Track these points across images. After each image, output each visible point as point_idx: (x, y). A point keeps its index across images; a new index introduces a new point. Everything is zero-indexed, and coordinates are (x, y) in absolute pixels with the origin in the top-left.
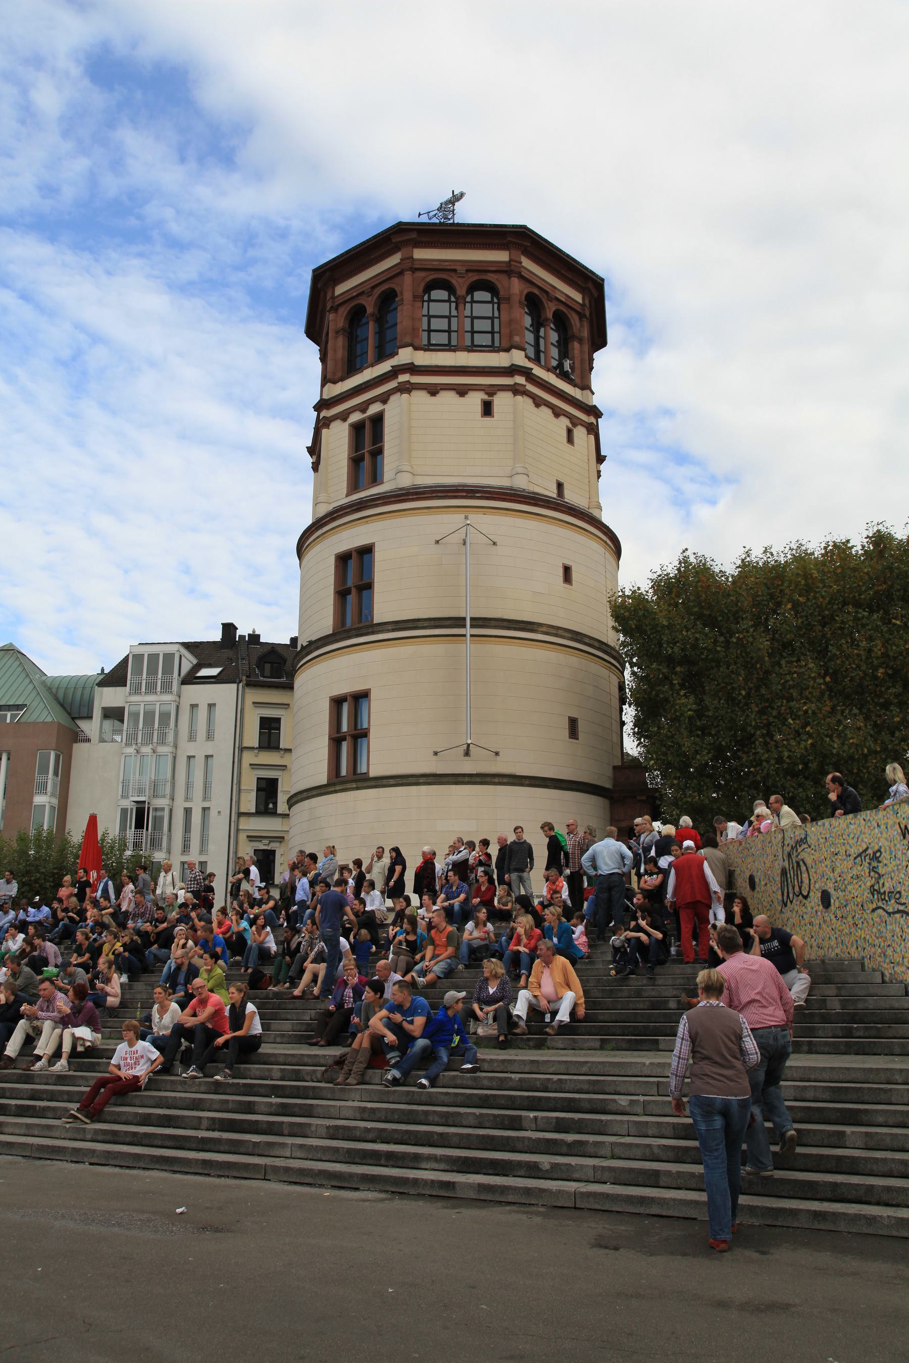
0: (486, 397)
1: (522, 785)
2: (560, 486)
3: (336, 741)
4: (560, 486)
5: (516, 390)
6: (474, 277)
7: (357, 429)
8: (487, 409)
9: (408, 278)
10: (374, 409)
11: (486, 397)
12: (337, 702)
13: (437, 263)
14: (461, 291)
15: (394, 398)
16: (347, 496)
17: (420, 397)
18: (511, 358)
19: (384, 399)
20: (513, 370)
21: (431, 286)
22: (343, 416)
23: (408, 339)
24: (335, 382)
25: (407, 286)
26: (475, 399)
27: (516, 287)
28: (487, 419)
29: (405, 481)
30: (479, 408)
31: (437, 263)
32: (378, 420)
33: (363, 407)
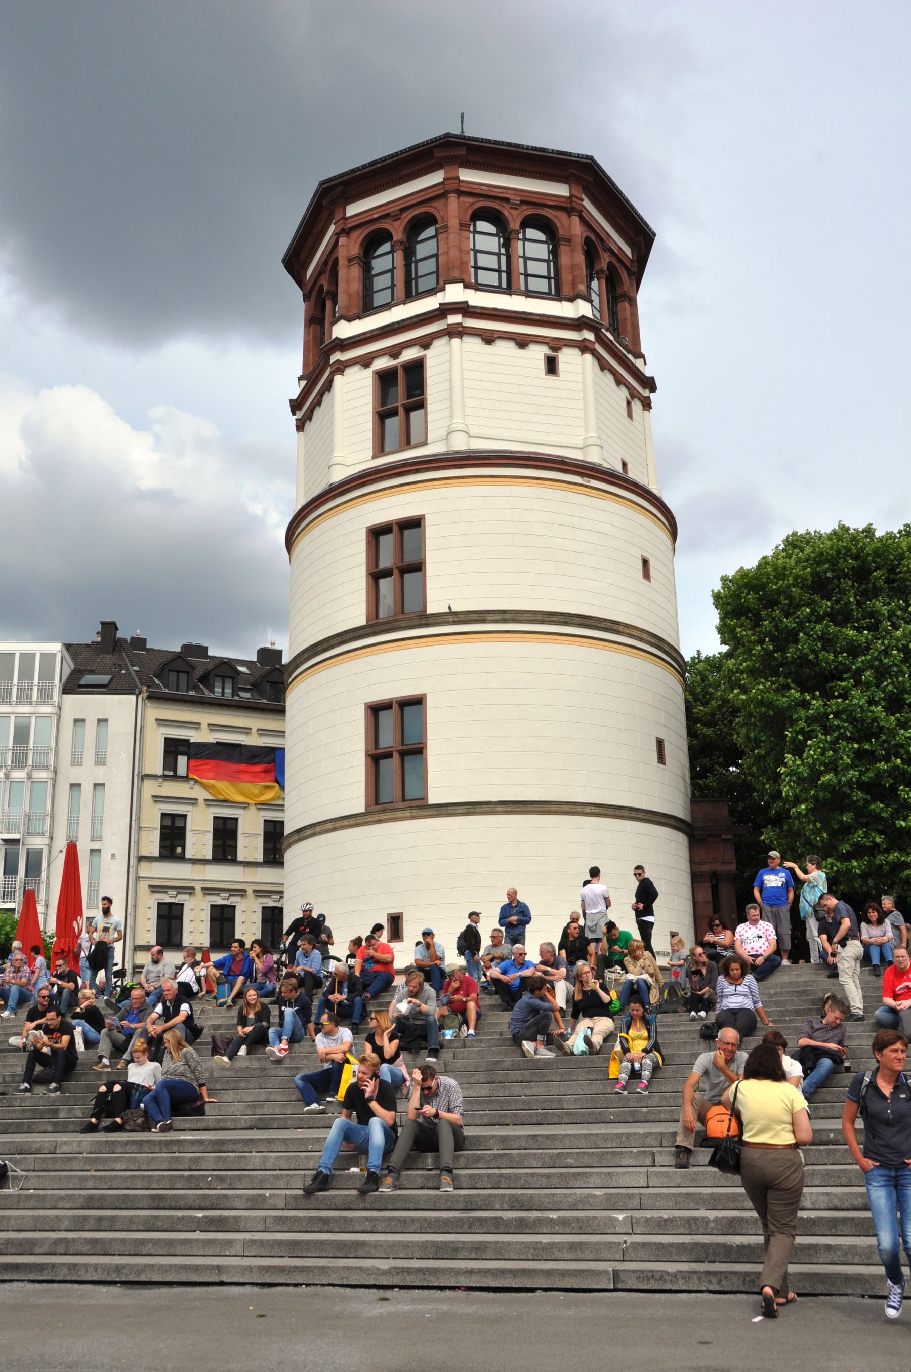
0: (550, 353)
1: (622, 817)
2: (624, 465)
3: (376, 758)
4: (624, 465)
5: (584, 347)
6: (531, 211)
7: (385, 379)
8: (551, 366)
9: (453, 202)
10: (410, 355)
11: (550, 353)
12: (375, 710)
13: (486, 188)
14: (514, 225)
15: (439, 345)
16: (374, 457)
17: (473, 344)
18: (577, 309)
19: (425, 343)
20: (579, 324)
21: (477, 216)
22: (365, 361)
23: (456, 274)
24: (349, 320)
25: (453, 210)
26: (538, 353)
28: (552, 377)
29: (460, 444)
30: (542, 365)
31: (486, 188)
32: (416, 369)
33: (394, 352)
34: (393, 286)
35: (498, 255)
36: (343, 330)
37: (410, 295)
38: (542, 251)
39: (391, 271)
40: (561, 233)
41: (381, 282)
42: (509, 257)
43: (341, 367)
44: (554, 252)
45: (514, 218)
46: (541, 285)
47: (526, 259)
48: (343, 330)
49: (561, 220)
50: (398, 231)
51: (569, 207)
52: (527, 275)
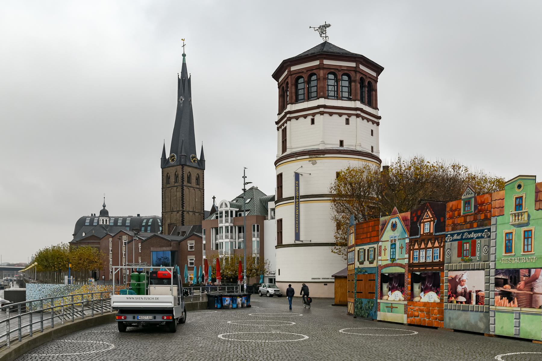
14: (339, 77)
27: (358, 76)
34: (304, 94)
35: (334, 86)
36: (290, 108)
37: (309, 99)
38: (346, 84)
39: (304, 89)
40: (352, 78)
41: (301, 92)
42: (337, 86)
43: (290, 119)
44: (350, 83)
45: (339, 74)
46: (346, 95)
47: (342, 86)
48: (290, 108)
49: (352, 74)
50: (306, 76)
51: (356, 70)
52: (342, 92)
